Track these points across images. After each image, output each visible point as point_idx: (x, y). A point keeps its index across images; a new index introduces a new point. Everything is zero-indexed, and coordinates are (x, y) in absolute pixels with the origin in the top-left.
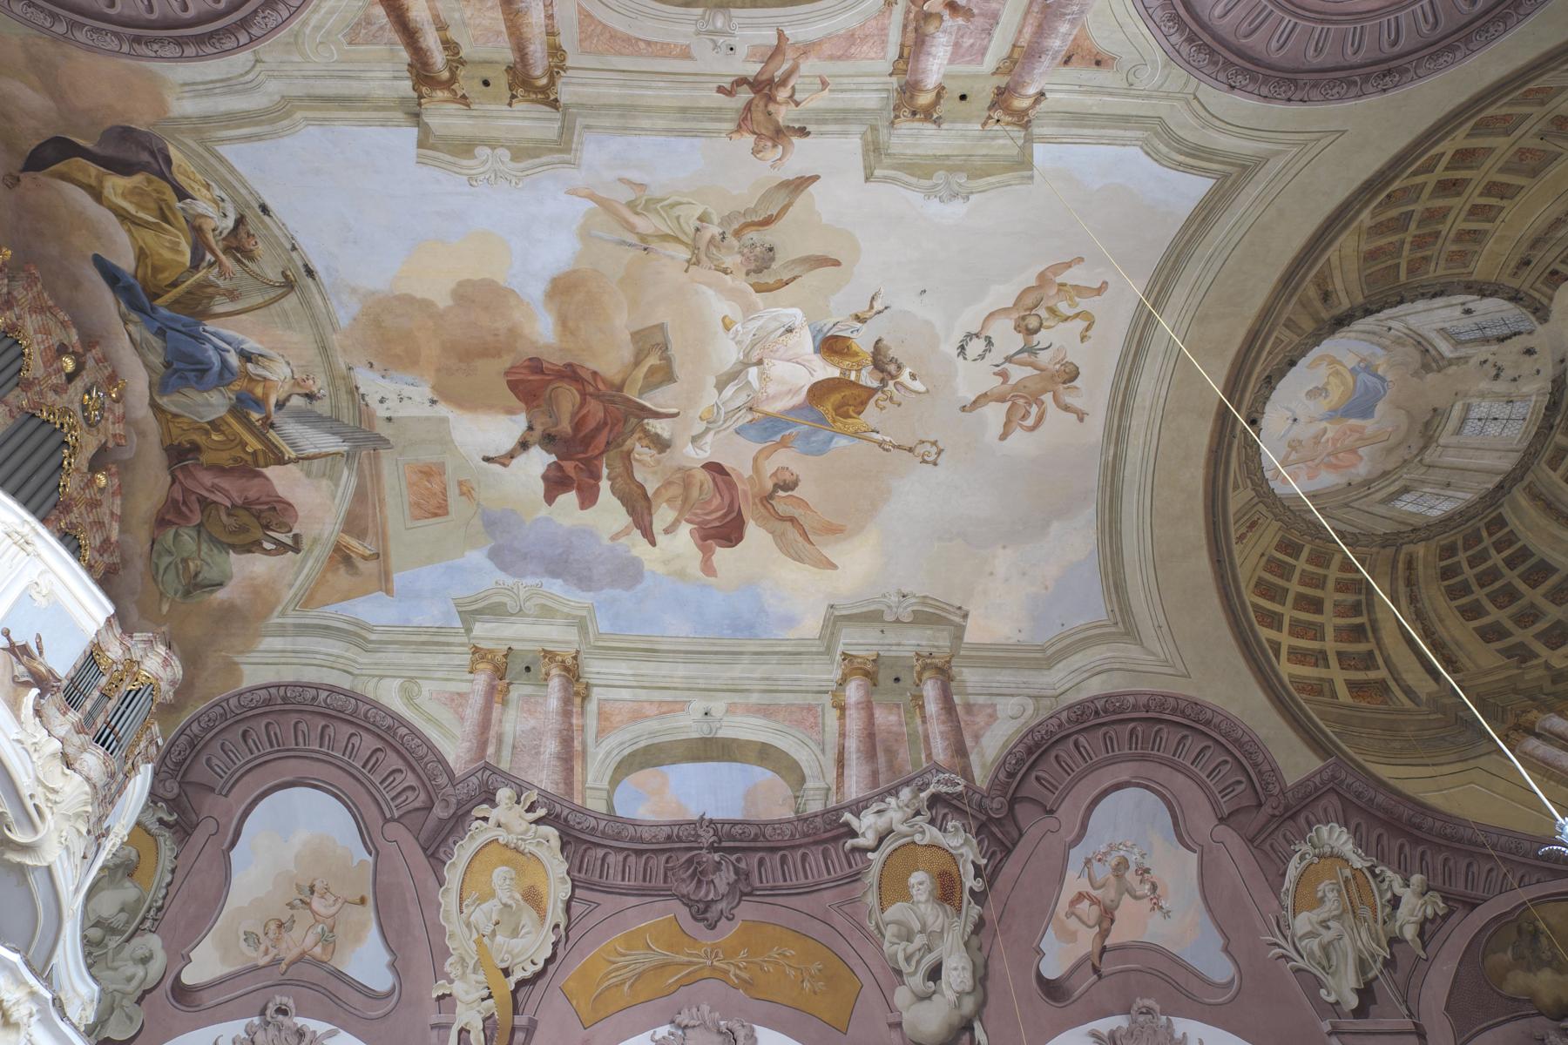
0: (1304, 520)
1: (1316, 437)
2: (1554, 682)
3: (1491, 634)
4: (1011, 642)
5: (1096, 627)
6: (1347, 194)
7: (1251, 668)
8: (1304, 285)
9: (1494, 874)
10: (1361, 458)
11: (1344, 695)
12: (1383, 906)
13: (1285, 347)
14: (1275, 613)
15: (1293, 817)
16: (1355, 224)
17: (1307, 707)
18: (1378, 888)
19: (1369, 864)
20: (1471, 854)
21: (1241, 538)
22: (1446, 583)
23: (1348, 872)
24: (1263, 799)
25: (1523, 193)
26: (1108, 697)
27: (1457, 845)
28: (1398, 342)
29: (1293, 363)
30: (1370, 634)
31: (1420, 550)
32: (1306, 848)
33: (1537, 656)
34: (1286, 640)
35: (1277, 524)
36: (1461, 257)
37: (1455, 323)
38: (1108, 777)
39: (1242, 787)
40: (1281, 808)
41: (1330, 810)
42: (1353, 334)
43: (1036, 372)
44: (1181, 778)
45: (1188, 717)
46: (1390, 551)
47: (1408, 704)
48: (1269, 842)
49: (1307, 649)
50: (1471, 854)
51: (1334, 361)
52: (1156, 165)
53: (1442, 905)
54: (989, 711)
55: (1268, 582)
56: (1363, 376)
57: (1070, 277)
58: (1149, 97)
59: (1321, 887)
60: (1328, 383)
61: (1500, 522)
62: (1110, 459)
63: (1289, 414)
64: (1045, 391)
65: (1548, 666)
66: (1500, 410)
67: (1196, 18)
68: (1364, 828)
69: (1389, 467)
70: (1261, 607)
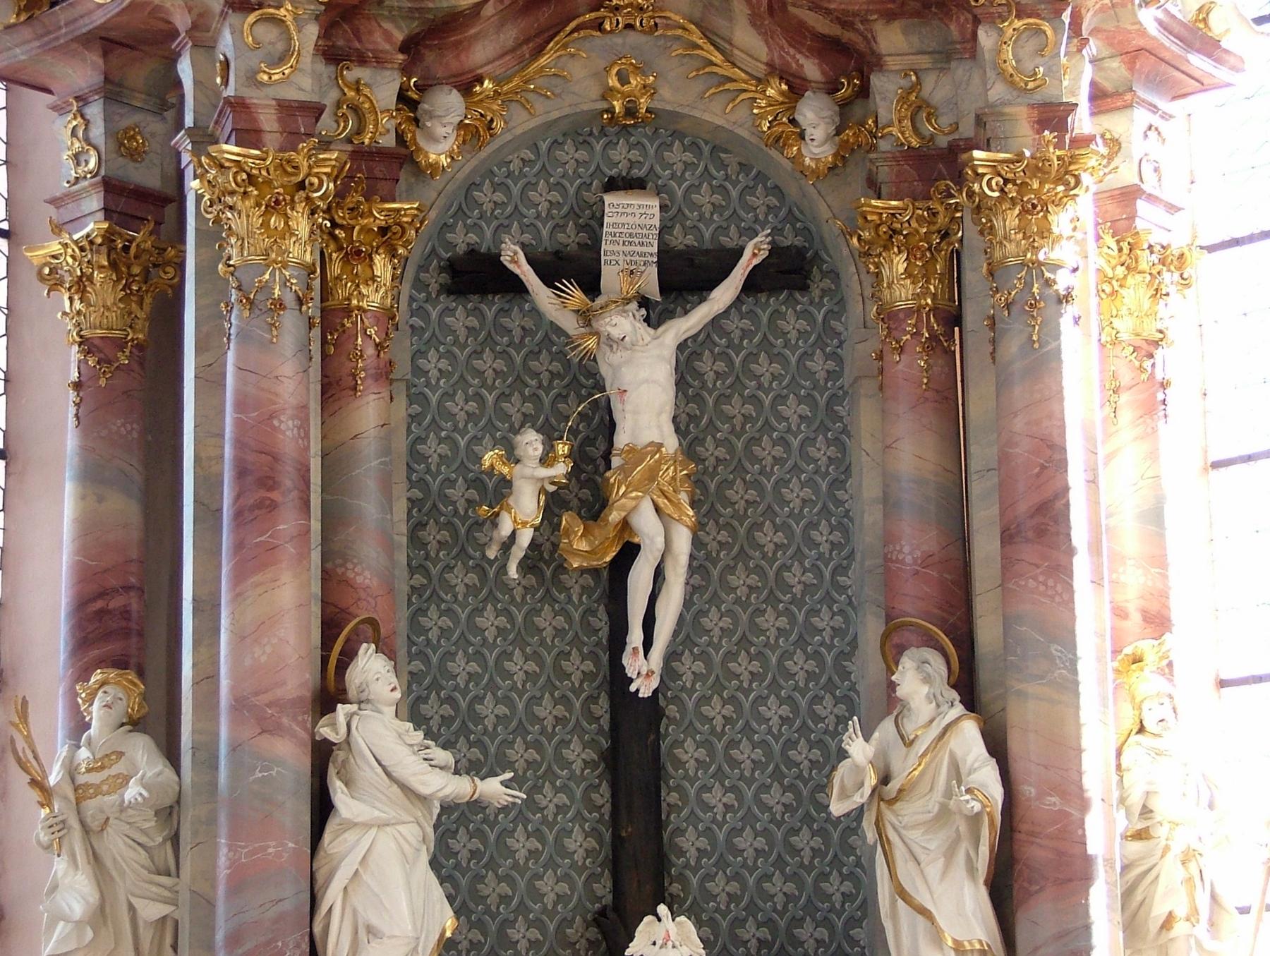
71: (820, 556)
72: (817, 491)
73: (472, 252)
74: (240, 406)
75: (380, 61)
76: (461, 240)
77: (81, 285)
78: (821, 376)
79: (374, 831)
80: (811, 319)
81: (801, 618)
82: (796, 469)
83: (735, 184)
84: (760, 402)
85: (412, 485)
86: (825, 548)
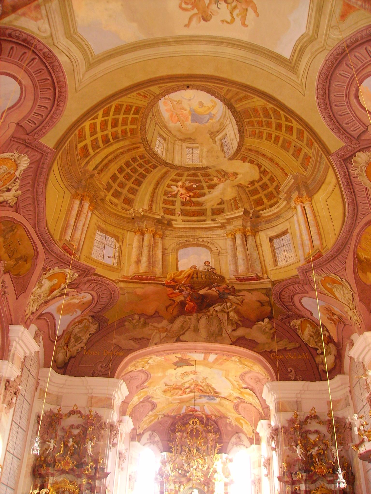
0: (149, 112)
1: (183, 108)
2: (101, 200)
3: (114, 178)
4: (77, 19)
5: (90, 52)
6: (280, 99)
7: (85, 113)
8: (245, 93)
9: (29, 211)
10: (176, 123)
11: (80, 145)
12: (6, 188)
13: (220, 91)
14: (109, 114)
15: (27, 146)
16: (268, 103)
17: (73, 135)
18: (12, 183)
19: (18, 177)
20: (34, 203)
21: (139, 94)
22: (130, 160)
23: (13, 172)
24: (31, 134)
25: (275, 145)
26: (60, 65)
27: (35, 198)
28: (221, 124)
29: (213, 94)
30: (106, 145)
31: (142, 149)
32: (17, 155)
33: (109, 192)
34: (99, 121)
35: (146, 104)
36: (253, 134)
37: (229, 137)
38: (22, 75)
39: (33, 125)
40: (29, 142)
41: (35, 157)
42: (225, 110)
43: (207, 5)
44: (31, 103)
45: (59, 97)
46: (140, 141)
47: (83, 164)
48: (15, 143)
49: (96, 128)
50: (34, 203)
51: (214, 107)
52: (297, 38)
53: (13, 203)
54: (39, 17)
55: (122, 108)
56: (208, 116)
57: (251, 14)
58: (326, 34)
59: (4, 166)
60: (205, 107)
61: (154, 167)
62: (168, 40)
63: (192, 98)
64: (198, 9)
65: (105, 196)
66: (196, 156)
67: (355, 47)
68: (32, 169)
69: (173, 132)
70: (110, 109)
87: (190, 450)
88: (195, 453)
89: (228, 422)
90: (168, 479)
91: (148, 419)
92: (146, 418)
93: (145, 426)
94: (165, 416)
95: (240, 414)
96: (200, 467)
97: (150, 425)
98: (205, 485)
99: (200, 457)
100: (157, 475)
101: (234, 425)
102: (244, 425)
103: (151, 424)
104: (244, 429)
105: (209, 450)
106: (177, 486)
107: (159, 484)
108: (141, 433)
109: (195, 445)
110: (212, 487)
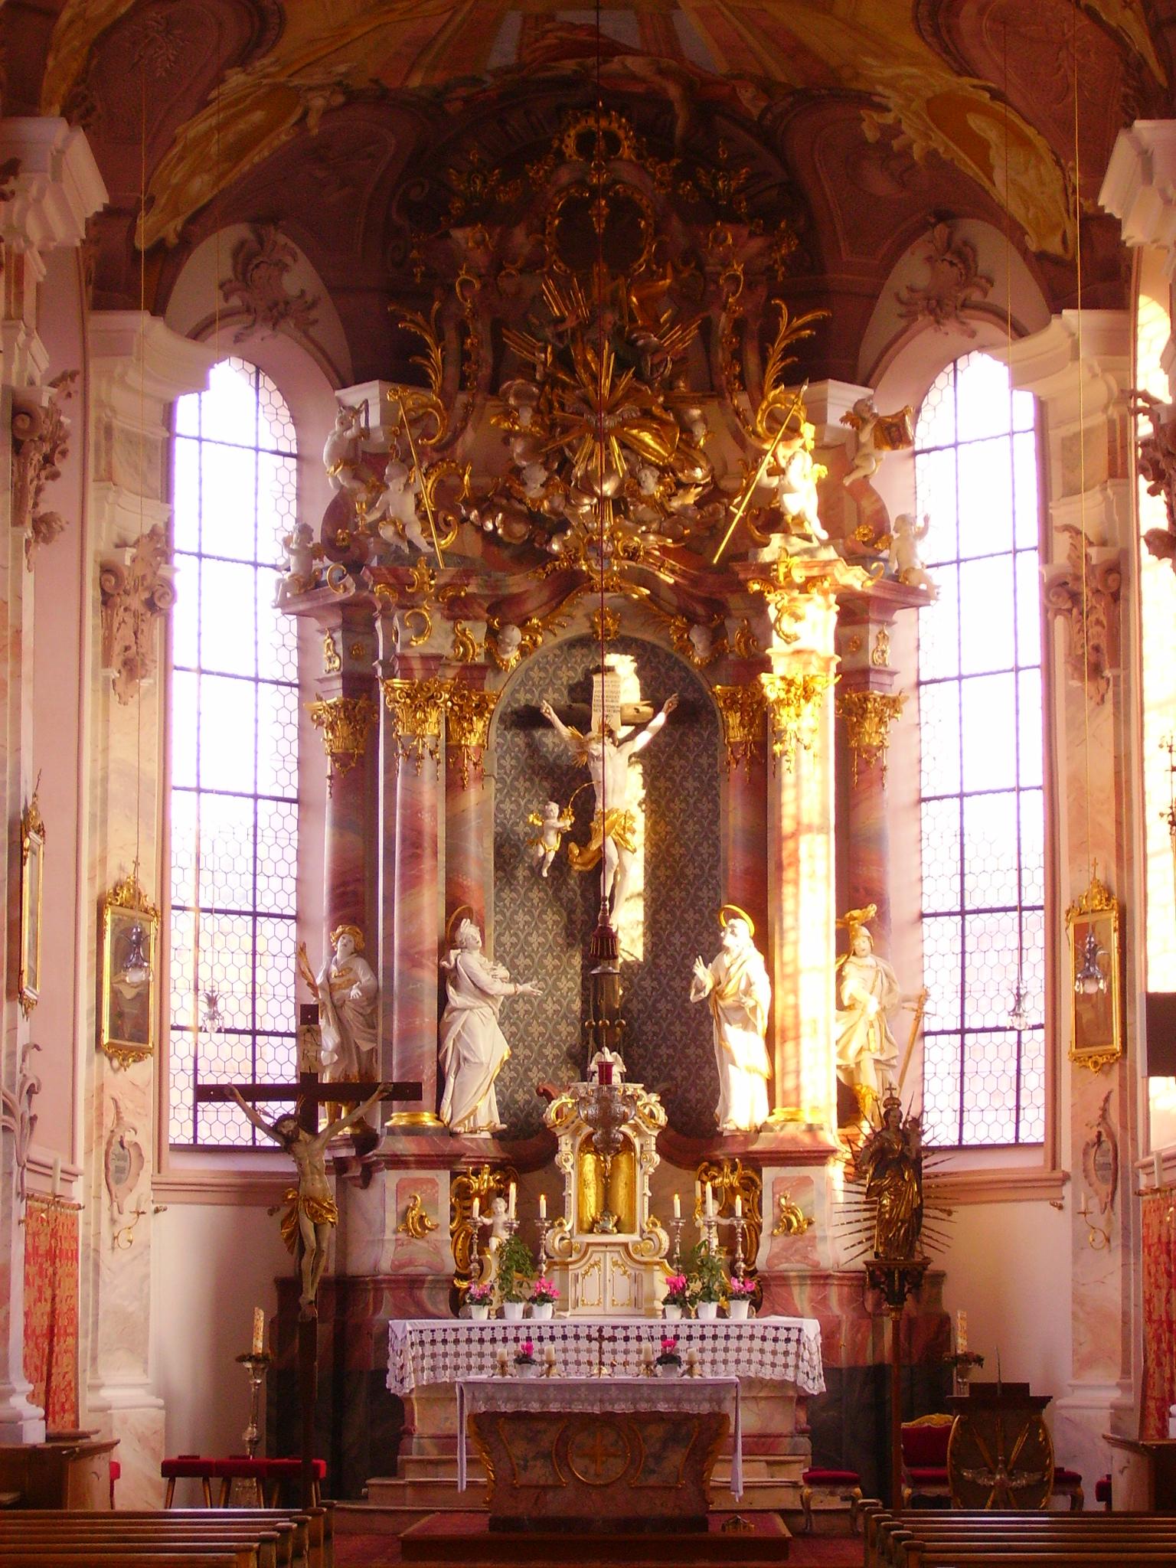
71: (703, 861)
72: (702, 827)
73: (526, 706)
74: (404, 807)
75: (477, 618)
76: (523, 698)
77: (332, 727)
78: (706, 766)
79: (468, 1012)
80: (701, 736)
81: (692, 891)
82: (691, 816)
83: (663, 665)
84: (675, 781)
85: (497, 825)
86: (705, 856)
87: (564, 360)
88: (606, 383)
89: (871, 135)
90: (400, 583)
91: (220, 127)
92: (199, 126)
93: (201, 188)
94: (353, 97)
95: (963, 68)
96: (652, 486)
97: (234, 175)
98: (692, 620)
99: (647, 414)
100: (316, 553)
101: (917, 153)
102: (995, 157)
103: (245, 166)
104: (1000, 190)
105: (721, 357)
106: (476, 633)
107: (336, 620)
108: (173, 240)
109: (610, 318)
110: (748, 635)
